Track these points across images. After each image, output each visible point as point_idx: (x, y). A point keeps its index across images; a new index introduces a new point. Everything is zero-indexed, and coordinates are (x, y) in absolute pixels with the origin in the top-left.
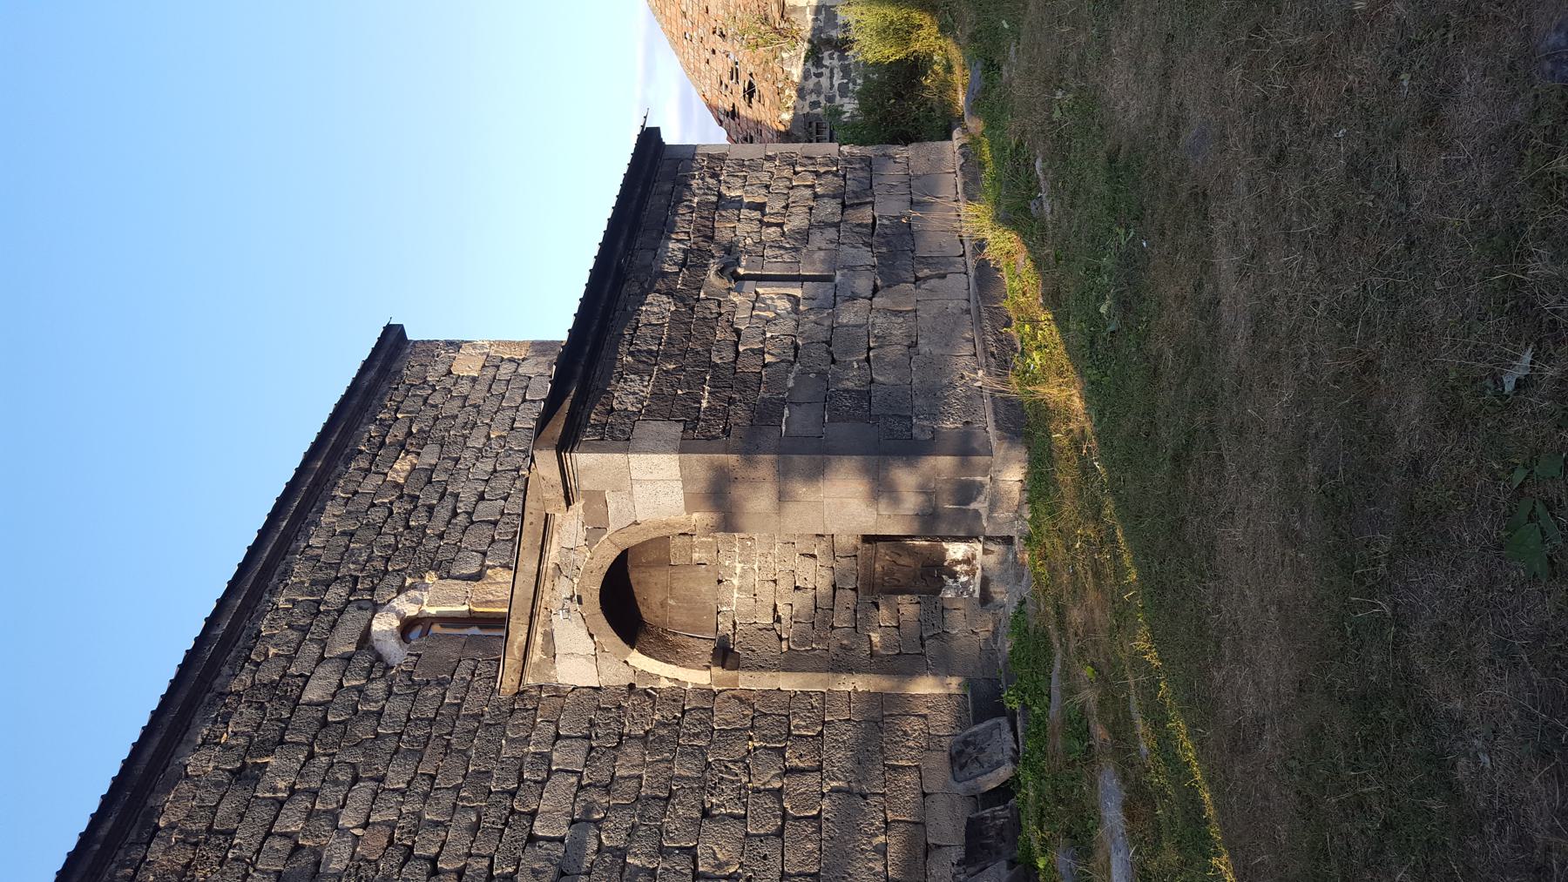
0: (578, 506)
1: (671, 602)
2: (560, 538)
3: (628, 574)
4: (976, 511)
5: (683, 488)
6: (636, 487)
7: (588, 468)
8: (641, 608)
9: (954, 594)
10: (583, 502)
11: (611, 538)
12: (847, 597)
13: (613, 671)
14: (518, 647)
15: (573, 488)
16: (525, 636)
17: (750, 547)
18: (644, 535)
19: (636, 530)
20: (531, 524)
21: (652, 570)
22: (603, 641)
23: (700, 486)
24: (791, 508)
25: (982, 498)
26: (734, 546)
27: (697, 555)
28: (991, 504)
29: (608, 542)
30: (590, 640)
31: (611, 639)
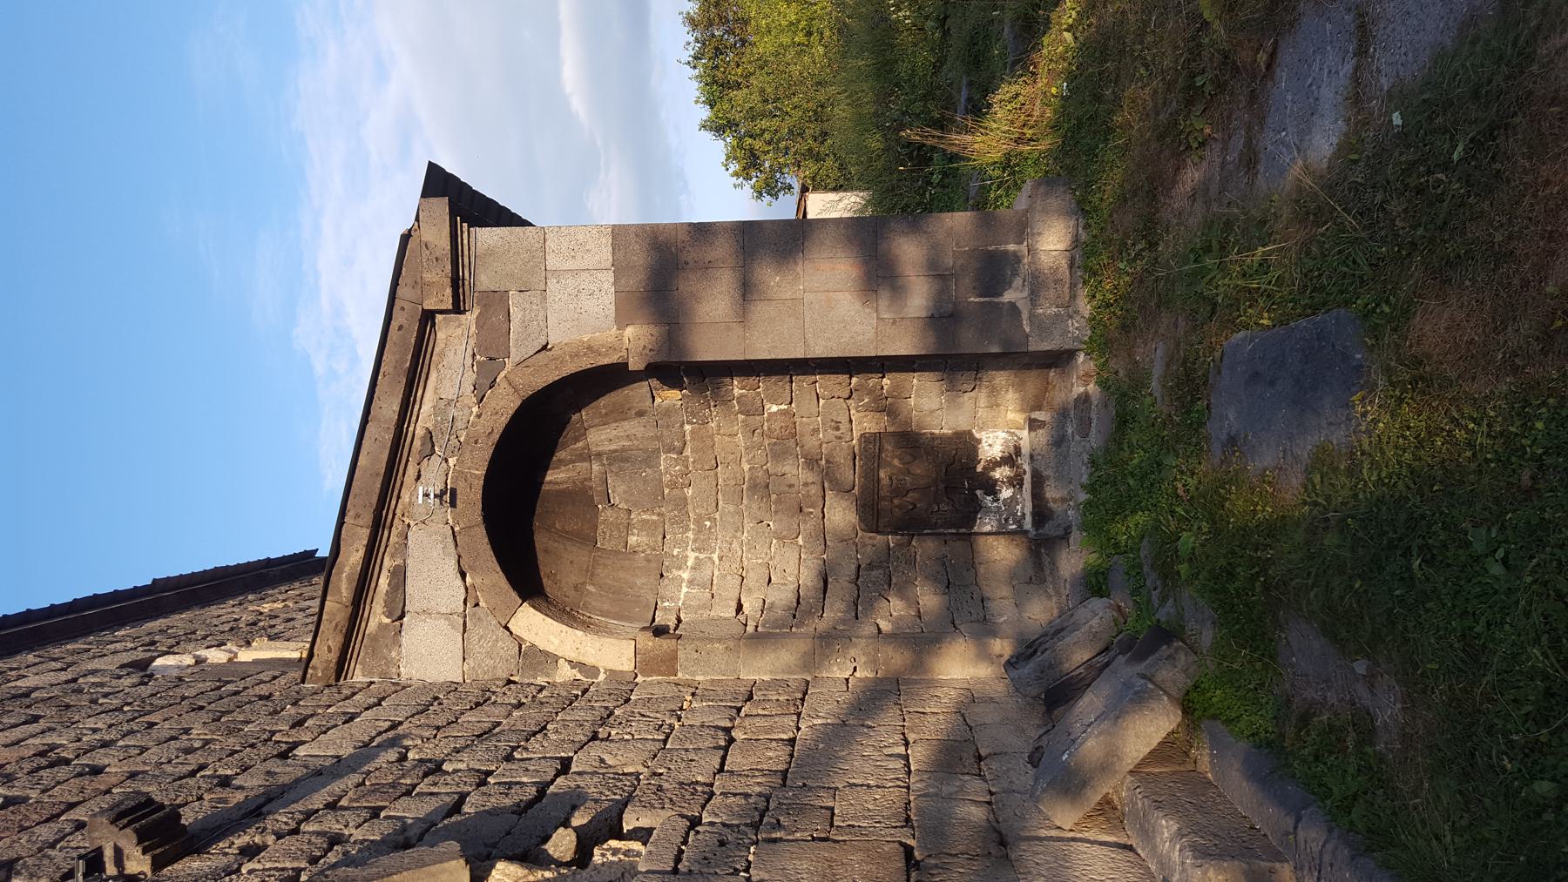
0: (470, 318)
1: (591, 588)
2: (440, 380)
3: (533, 534)
4: (1013, 306)
5: (615, 284)
6: (552, 283)
7: (490, 252)
8: (545, 580)
9: (994, 523)
10: (477, 311)
11: (511, 377)
12: (841, 587)
13: (488, 646)
14: (349, 578)
15: (467, 283)
16: (361, 553)
17: (710, 528)
18: (556, 367)
19: (546, 361)
20: (400, 328)
21: (568, 544)
22: (478, 581)
23: (636, 280)
24: (760, 311)
25: (1018, 282)
26: (687, 529)
27: (635, 538)
28: (1032, 292)
29: (505, 384)
30: (459, 582)
31: (491, 577)
